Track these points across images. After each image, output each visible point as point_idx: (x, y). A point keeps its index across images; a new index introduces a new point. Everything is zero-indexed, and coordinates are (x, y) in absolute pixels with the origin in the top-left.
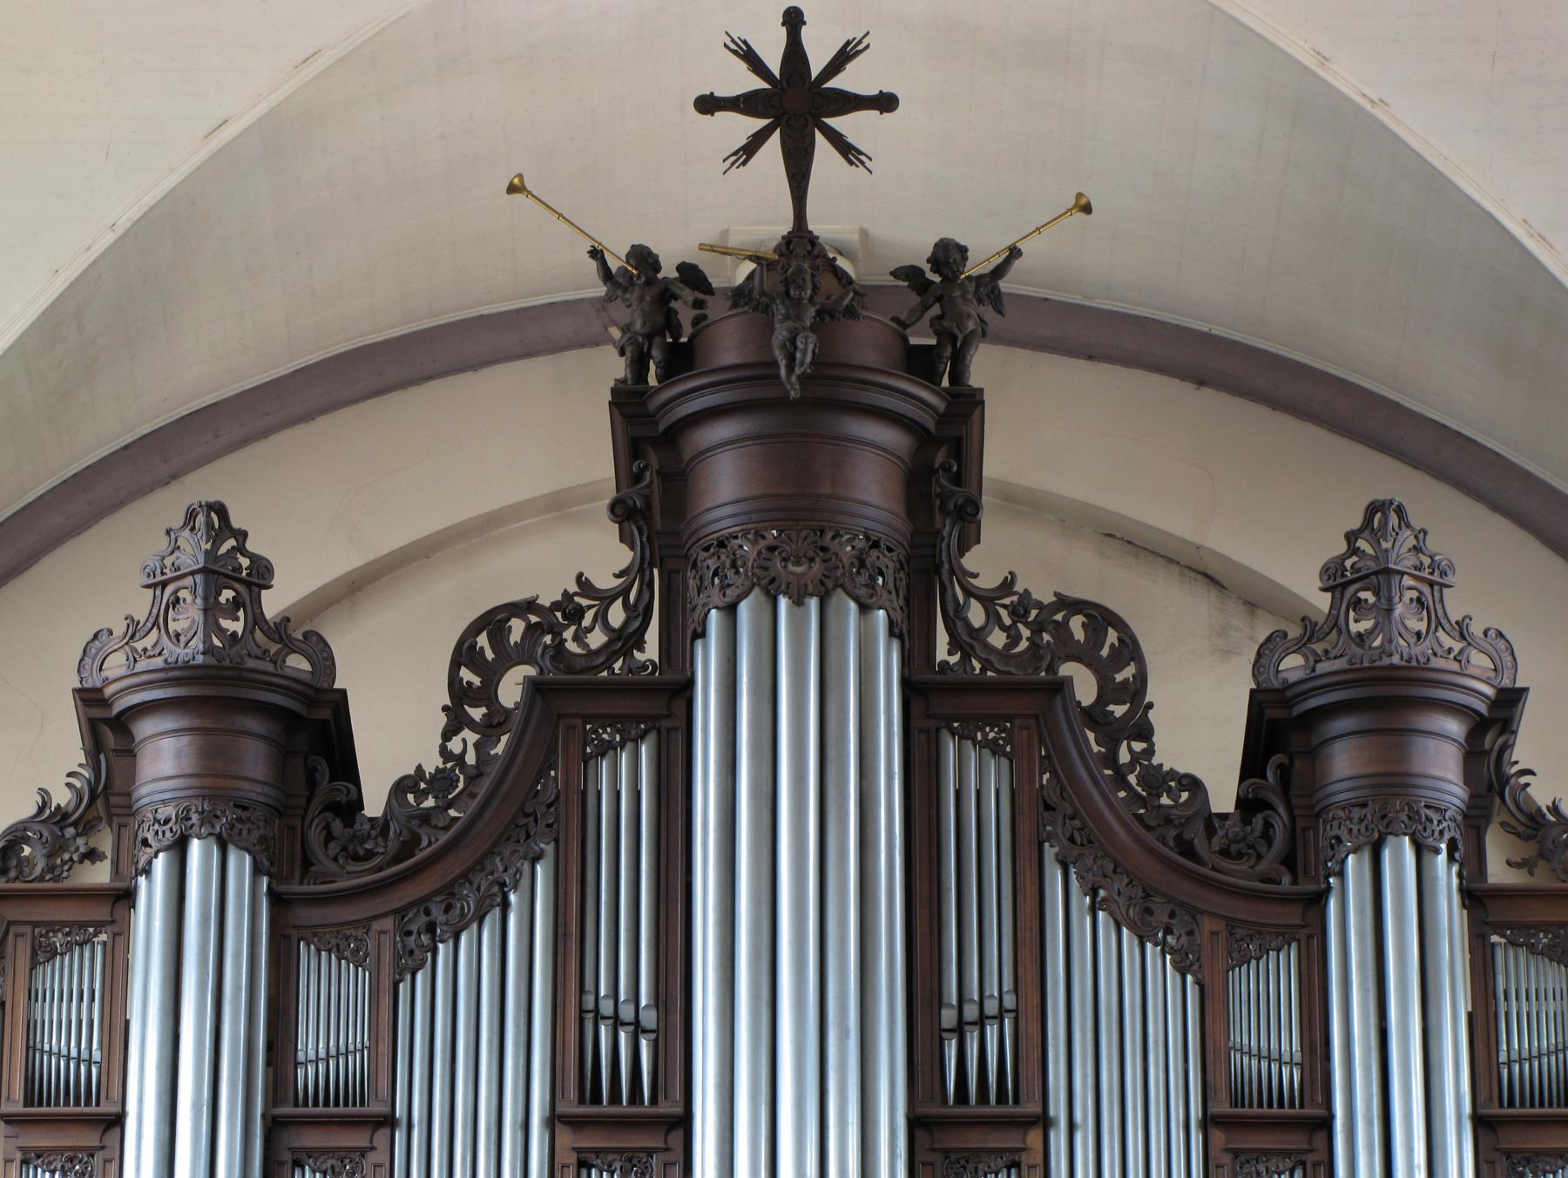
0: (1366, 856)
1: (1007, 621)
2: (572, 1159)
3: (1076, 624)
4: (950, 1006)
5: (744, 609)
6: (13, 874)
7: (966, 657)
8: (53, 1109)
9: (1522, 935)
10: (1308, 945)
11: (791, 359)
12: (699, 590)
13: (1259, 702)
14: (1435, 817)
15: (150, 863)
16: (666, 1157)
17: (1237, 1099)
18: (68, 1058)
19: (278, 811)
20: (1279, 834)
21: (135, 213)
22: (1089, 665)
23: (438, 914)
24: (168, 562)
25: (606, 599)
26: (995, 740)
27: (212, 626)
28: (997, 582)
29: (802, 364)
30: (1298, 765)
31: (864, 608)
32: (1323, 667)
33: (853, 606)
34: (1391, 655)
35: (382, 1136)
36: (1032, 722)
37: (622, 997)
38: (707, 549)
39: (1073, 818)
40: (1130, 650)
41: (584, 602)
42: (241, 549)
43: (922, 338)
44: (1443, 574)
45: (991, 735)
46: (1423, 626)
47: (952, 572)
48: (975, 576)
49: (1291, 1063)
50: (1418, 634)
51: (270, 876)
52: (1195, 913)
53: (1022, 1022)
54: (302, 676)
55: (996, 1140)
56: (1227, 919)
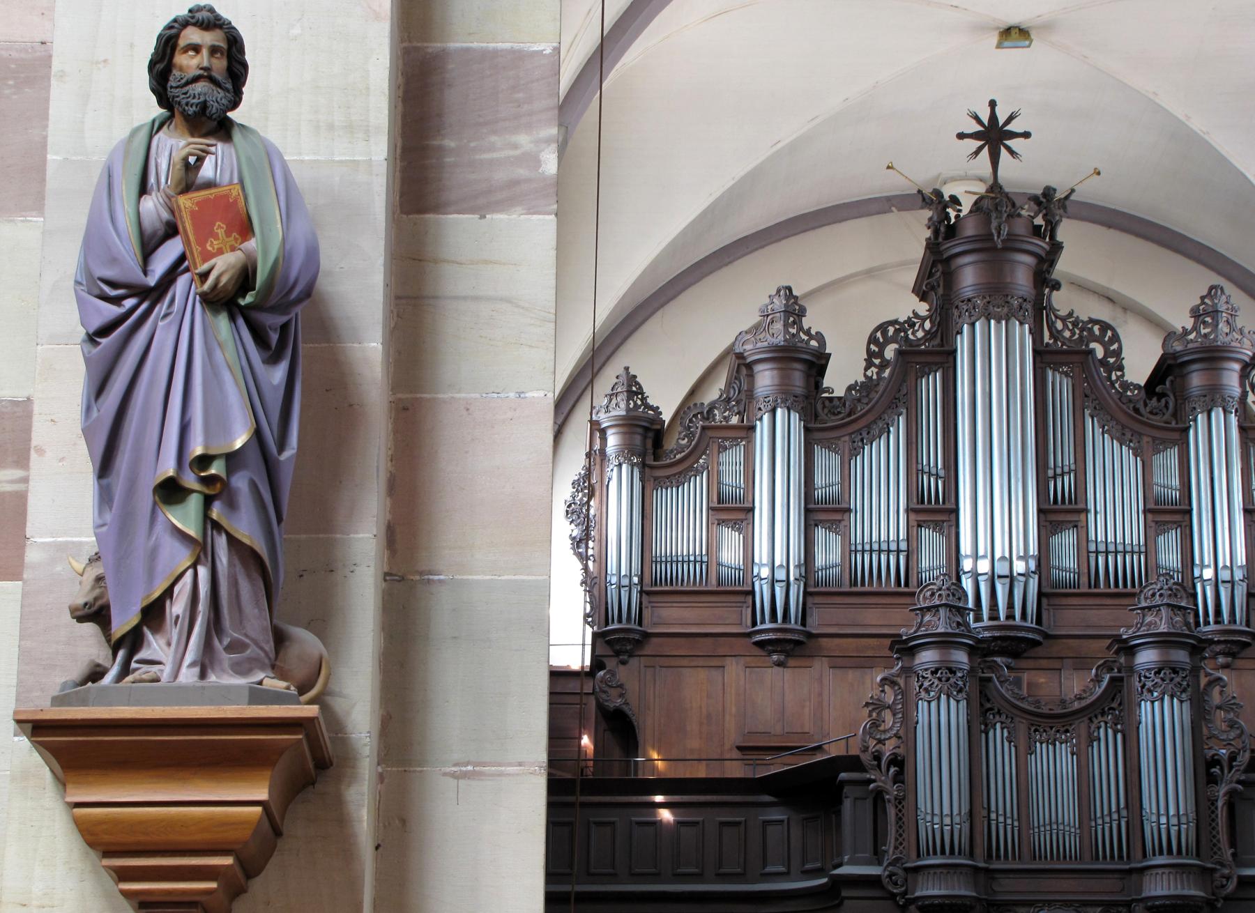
0: (1205, 414)
1: (1071, 327)
2: (915, 524)
3: (1096, 329)
4: (1051, 468)
5: (978, 325)
6: (711, 420)
7: (1056, 341)
8: (727, 505)
10: (1182, 448)
11: (999, 234)
12: (959, 317)
14: (1231, 400)
15: (762, 417)
16: (950, 523)
17: (1156, 503)
18: (732, 487)
19: (807, 397)
20: (1171, 405)
21: (742, 174)
22: (1101, 344)
23: (864, 434)
24: (769, 307)
25: (923, 319)
26: (1067, 371)
27: (787, 332)
28: (1067, 313)
29: (1003, 235)
30: (1178, 380)
31: (1021, 324)
32: (1190, 346)
33: (1017, 322)
34: (1217, 342)
35: (847, 514)
36: (1080, 365)
37: (932, 465)
38: (963, 302)
39: (1095, 400)
40: (1116, 338)
41: (916, 320)
42: (796, 303)
43: (1039, 221)
44: (1236, 311)
45: (1065, 370)
46: (1228, 331)
47: (1050, 309)
48: (1059, 311)
49: (1176, 490)
50: (1227, 334)
51: (804, 421)
52: (1140, 434)
53: (1078, 474)
54: (816, 348)
55: (1069, 517)
56: (1153, 437)
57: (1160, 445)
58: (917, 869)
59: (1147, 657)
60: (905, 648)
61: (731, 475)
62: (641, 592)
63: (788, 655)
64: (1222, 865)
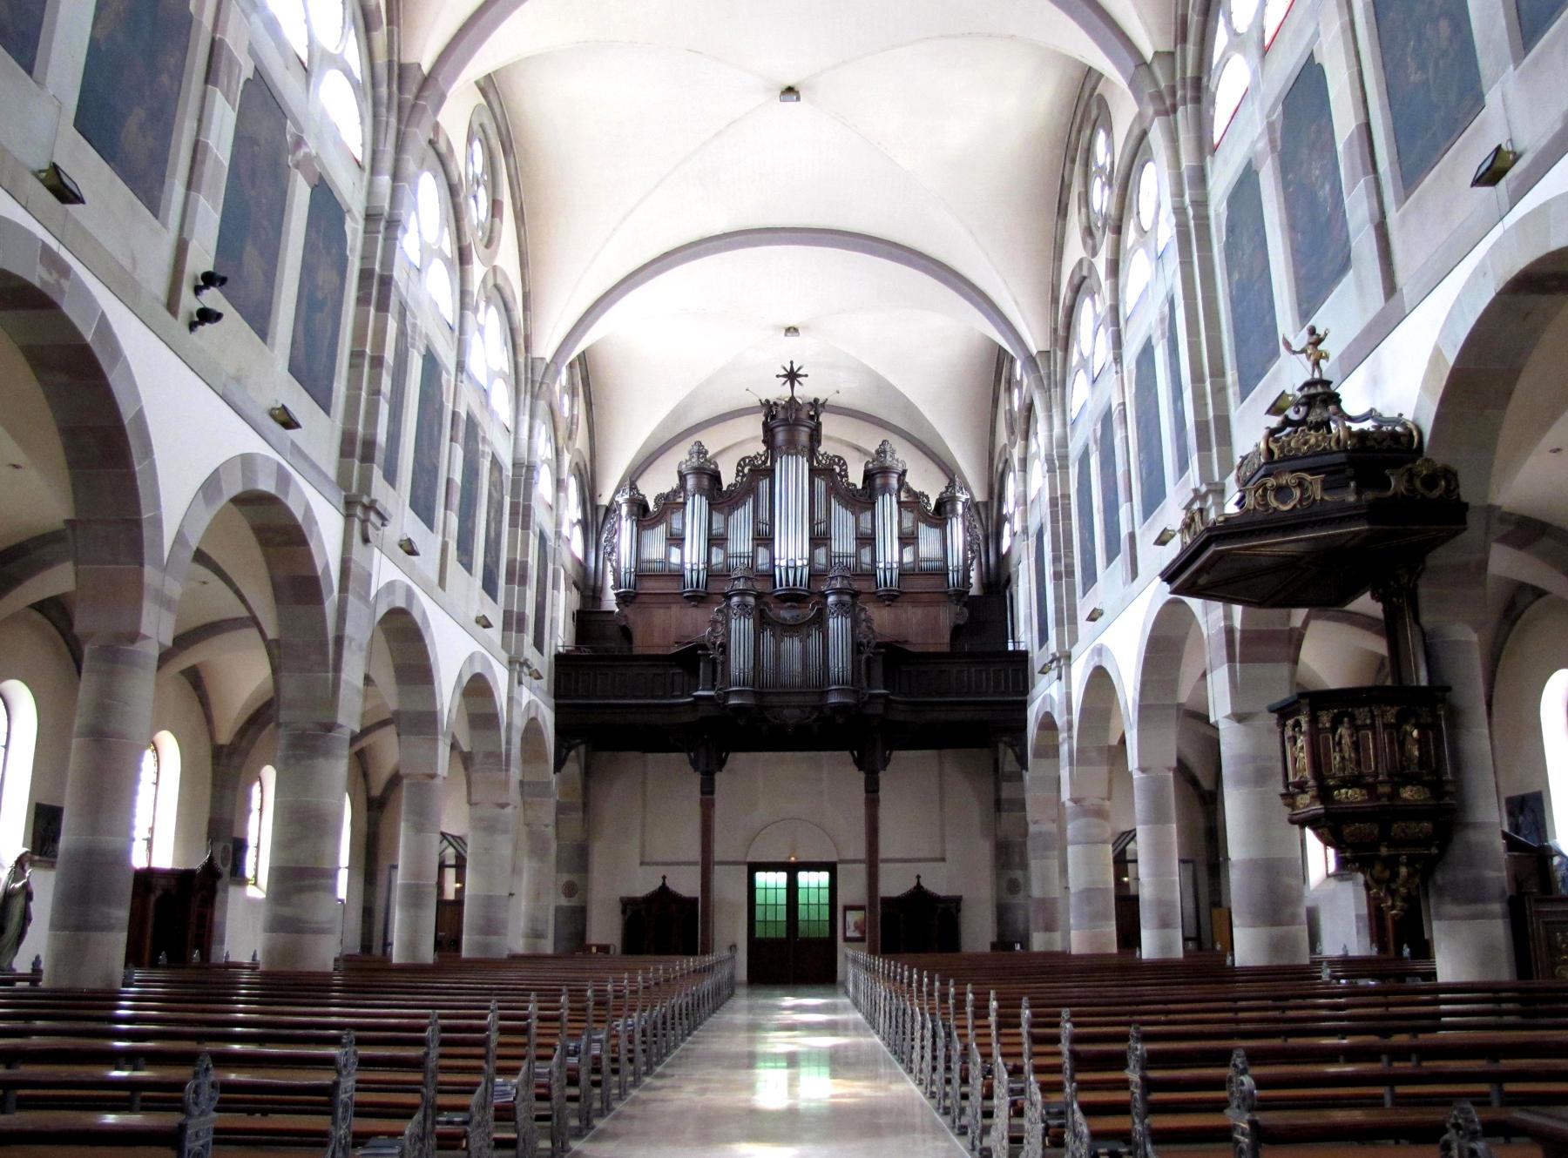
9: (906, 509)
13: (865, 472)
25: (761, 456)
40: (845, 463)
43: (812, 413)
57: (863, 510)
58: (729, 692)
59: (831, 599)
60: (728, 597)
61: (676, 524)
62: (636, 575)
63: (699, 602)
64: (862, 689)
